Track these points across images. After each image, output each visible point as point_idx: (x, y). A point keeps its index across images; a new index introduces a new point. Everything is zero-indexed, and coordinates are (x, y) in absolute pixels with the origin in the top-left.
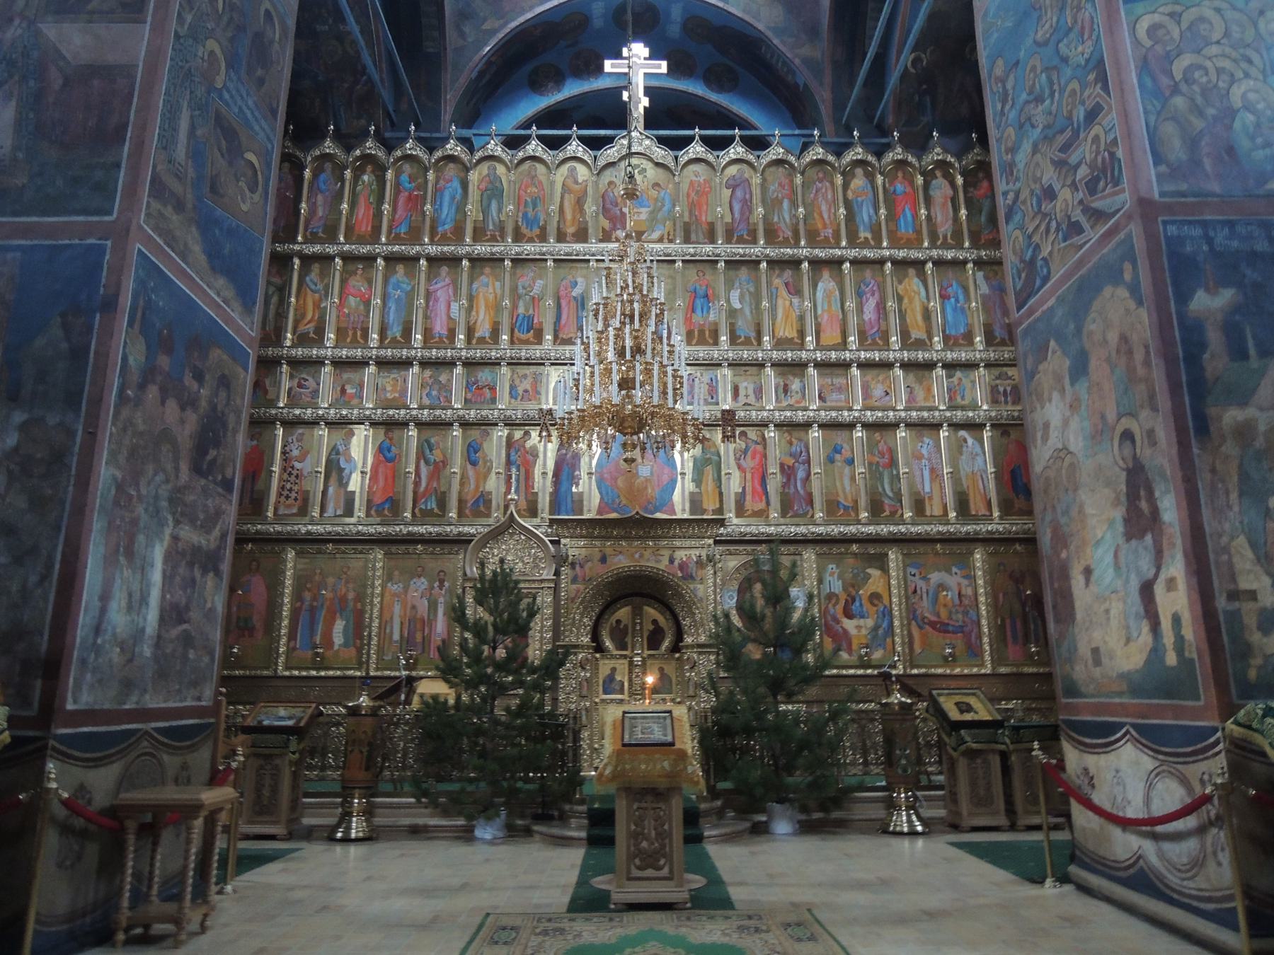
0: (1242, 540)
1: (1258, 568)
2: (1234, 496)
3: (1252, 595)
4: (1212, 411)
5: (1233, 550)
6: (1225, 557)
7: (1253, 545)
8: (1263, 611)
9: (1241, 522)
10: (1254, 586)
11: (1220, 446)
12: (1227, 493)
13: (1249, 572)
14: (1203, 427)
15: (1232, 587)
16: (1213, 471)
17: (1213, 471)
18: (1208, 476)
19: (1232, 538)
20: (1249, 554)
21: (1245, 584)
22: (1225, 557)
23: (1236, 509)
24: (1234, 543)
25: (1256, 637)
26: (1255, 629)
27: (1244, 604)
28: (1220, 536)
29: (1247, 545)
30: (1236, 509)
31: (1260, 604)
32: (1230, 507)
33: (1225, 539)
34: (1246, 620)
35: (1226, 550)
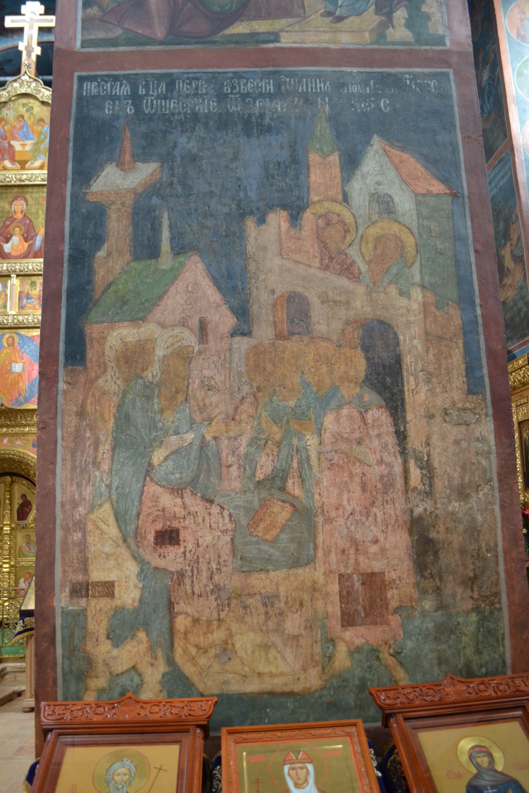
0: (106, 511)
1: (124, 551)
2: (105, 448)
3: (108, 589)
4: (93, 330)
5: (90, 526)
6: (77, 536)
7: (120, 518)
8: (118, 611)
9: (109, 486)
10: (113, 577)
11: (97, 377)
12: (97, 444)
13: (108, 556)
14: (77, 353)
15: (80, 577)
16: (81, 414)
17: (81, 414)
18: (74, 421)
19: (92, 509)
20: (113, 531)
21: (97, 575)
22: (77, 536)
23: (105, 466)
24: (92, 517)
25: (102, 650)
26: (103, 638)
27: (93, 602)
28: (75, 504)
29: (112, 520)
30: (105, 466)
31: (118, 602)
32: (96, 464)
33: (81, 510)
34: (91, 626)
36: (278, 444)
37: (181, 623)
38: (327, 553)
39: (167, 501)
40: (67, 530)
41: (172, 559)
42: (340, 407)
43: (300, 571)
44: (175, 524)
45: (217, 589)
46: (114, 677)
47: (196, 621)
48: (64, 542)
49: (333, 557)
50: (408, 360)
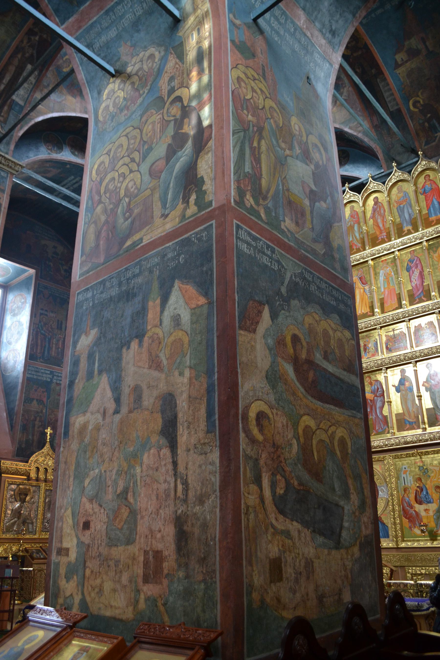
0: (69, 512)
20: (70, 521)
21: (65, 545)
24: (65, 514)
33: (63, 511)
35: (62, 518)
36: (126, 473)
37: (88, 572)
38: (140, 538)
39: (88, 506)
40: (58, 521)
41: (86, 538)
42: (150, 449)
43: (129, 547)
44: (89, 519)
45: (100, 555)
46: (66, 598)
47: (92, 572)
48: (57, 527)
49: (142, 540)
50: (180, 415)
